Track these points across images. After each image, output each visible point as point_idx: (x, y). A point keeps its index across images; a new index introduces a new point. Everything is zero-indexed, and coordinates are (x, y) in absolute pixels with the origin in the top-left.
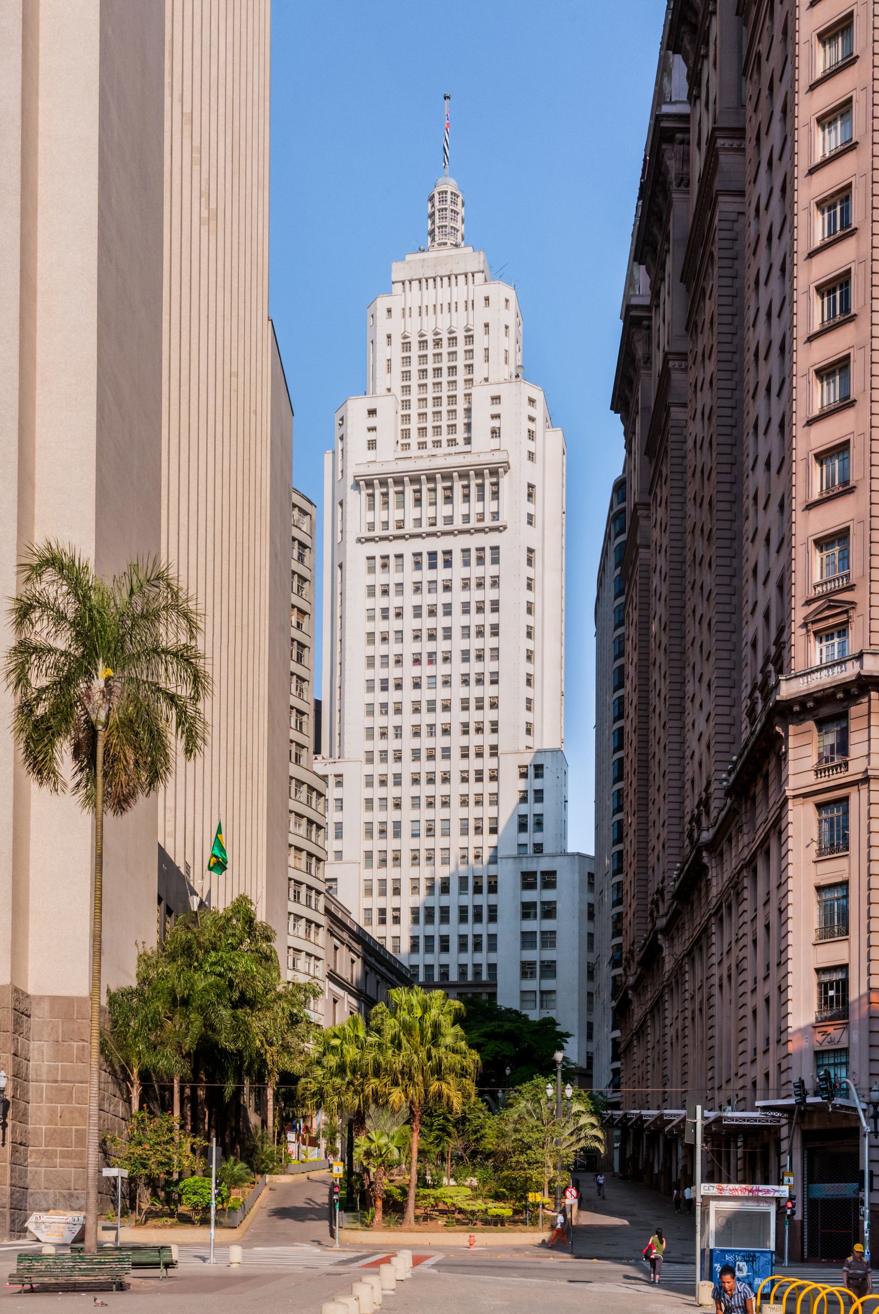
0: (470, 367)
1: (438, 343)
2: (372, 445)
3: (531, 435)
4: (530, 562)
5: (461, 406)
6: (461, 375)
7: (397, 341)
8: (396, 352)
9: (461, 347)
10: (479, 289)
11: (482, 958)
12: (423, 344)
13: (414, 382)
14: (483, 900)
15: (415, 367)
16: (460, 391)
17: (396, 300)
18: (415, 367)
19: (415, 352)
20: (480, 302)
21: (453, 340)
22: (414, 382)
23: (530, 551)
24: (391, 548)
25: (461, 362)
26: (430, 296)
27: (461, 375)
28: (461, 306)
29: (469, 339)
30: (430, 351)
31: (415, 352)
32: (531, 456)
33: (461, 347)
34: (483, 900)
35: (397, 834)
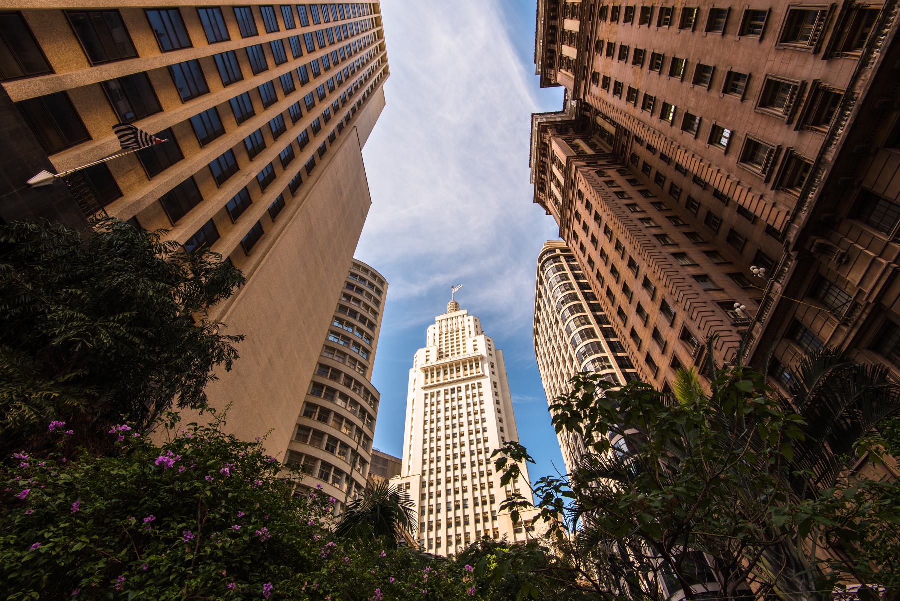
2: (427, 360)
4: (495, 387)
5: (462, 347)
6: (461, 339)
13: (444, 343)
15: (444, 340)
16: (461, 343)
17: (437, 325)
18: (444, 340)
19: (444, 336)
22: (444, 343)
23: (495, 383)
24: (435, 390)
25: (461, 336)
27: (461, 339)
30: (450, 335)
31: (444, 336)
33: (461, 332)
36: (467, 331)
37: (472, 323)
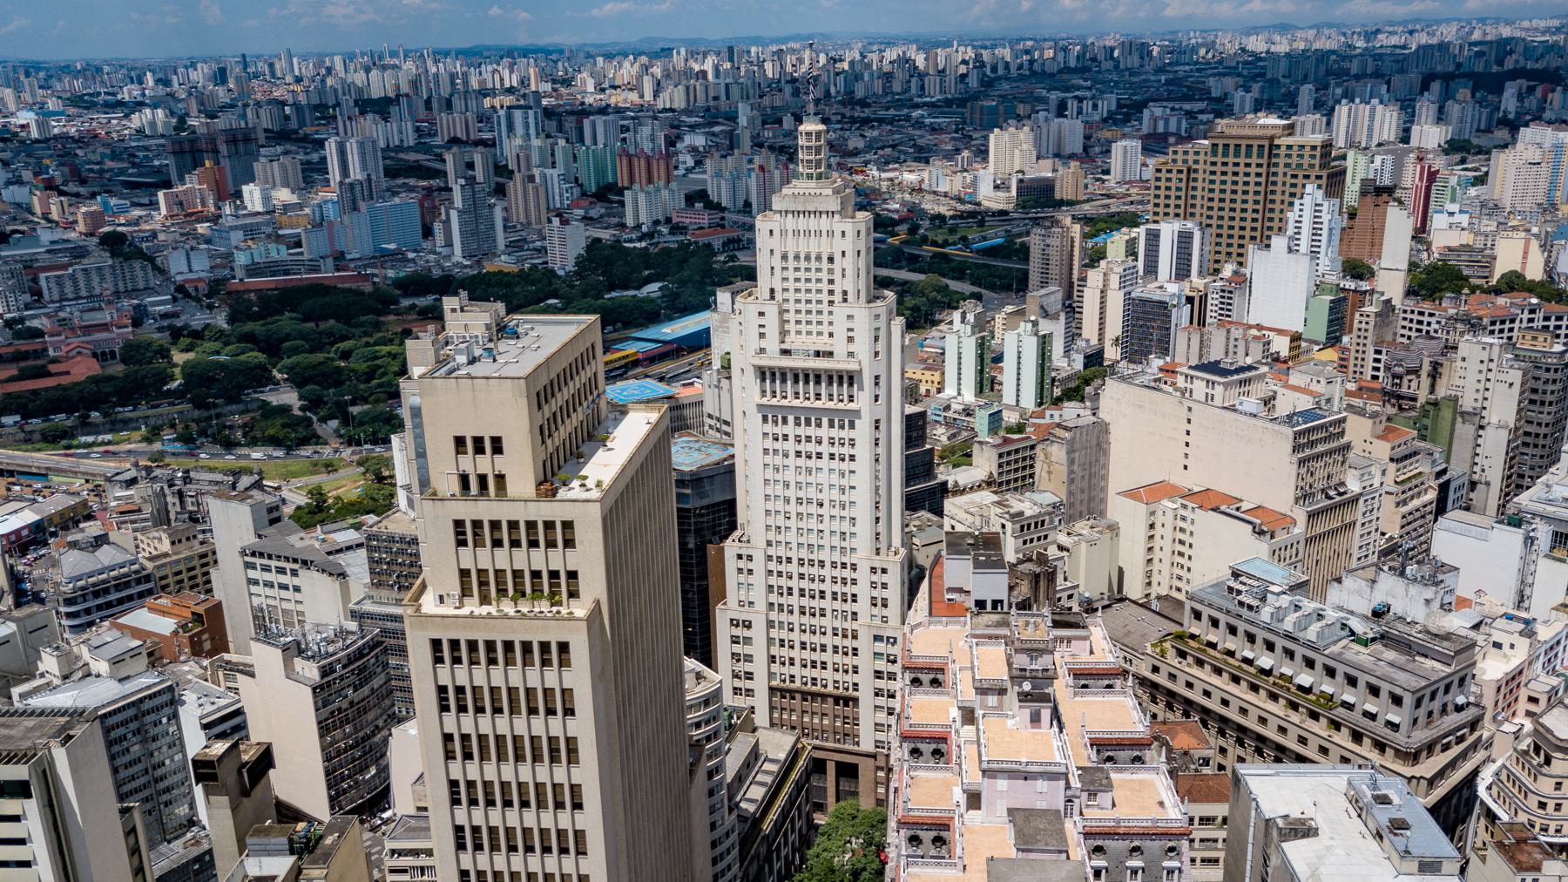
0: (831, 282)
1: (808, 258)
2: (762, 335)
3: (876, 339)
7: (778, 255)
8: (777, 262)
9: (825, 265)
10: (839, 224)
11: (848, 678)
12: (797, 257)
14: (848, 643)
19: (791, 264)
20: (838, 234)
21: (819, 258)
23: (877, 421)
26: (802, 223)
28: (824, 234)
29: (831, 260)
31: (791, 264)
32: (877, 354)
34: (848, 643)
35: (790, 594)
36: (837, 266)
37: (848, 244)
